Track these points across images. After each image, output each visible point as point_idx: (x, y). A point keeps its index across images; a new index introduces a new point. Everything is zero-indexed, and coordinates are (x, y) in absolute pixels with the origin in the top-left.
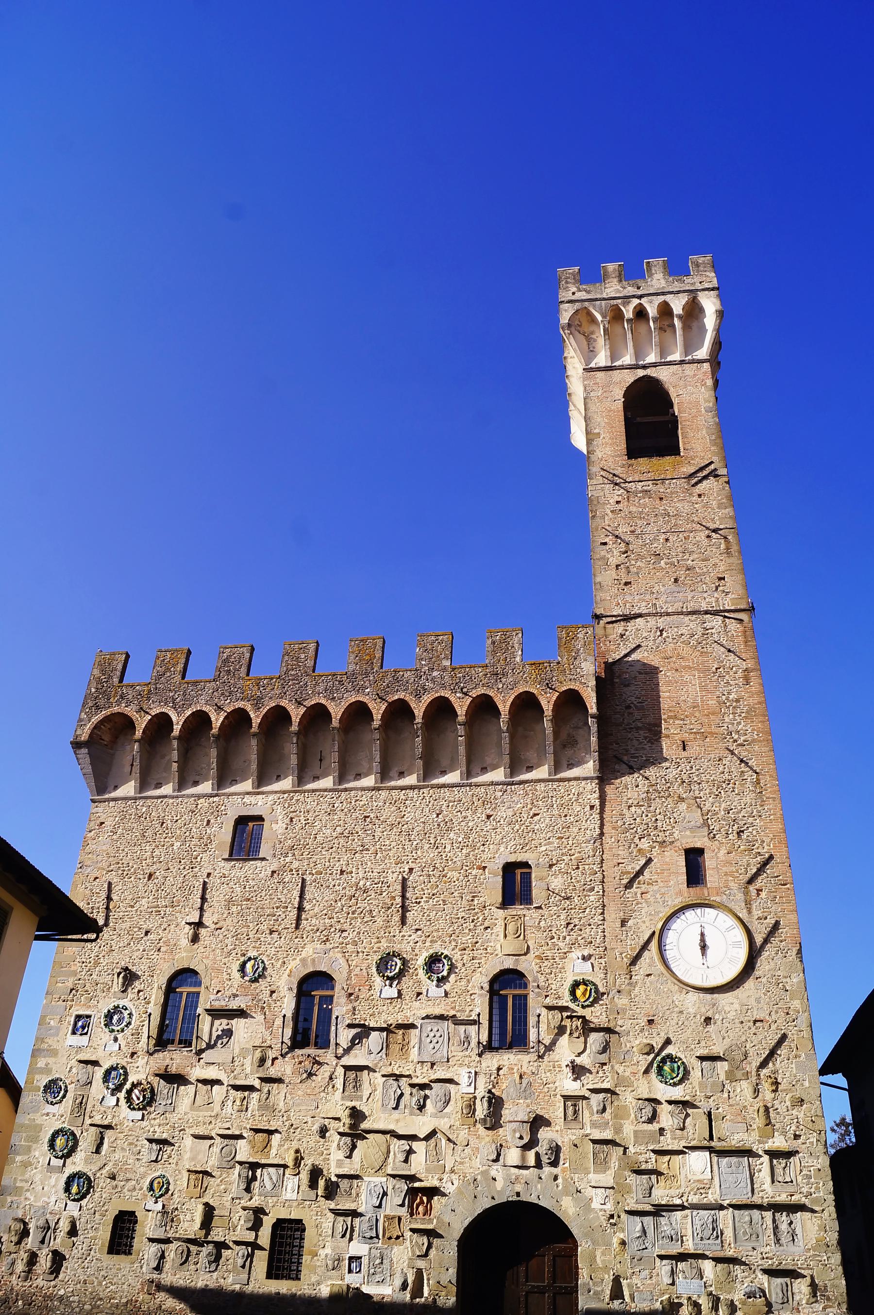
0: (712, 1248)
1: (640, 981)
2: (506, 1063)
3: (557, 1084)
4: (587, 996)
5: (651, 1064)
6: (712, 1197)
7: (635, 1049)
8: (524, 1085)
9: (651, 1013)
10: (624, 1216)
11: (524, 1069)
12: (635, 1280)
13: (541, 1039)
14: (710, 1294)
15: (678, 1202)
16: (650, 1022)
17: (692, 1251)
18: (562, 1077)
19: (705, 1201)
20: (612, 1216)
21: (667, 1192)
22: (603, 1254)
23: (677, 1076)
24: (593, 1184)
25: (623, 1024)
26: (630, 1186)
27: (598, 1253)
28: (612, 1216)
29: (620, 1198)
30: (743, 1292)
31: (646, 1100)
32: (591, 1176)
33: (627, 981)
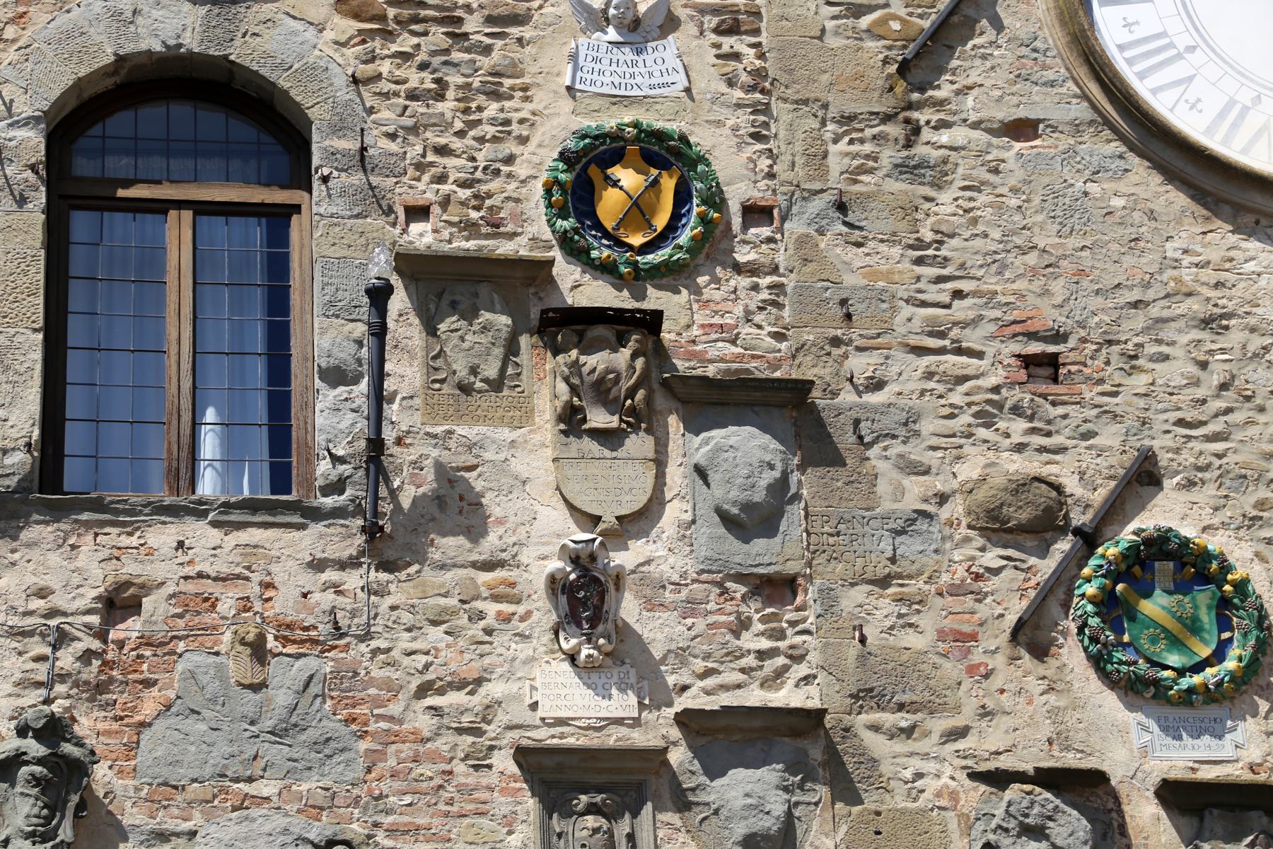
1: (964, 168)
2: (164, 570)
3: (494, 689)
4: (661, 221)
5: (1059, 589)
7: (956, 508)
8: (281, 697)
9: (1049, 317)
11: (284, 604)
13: (388, 434)
16: (1043, 367)
18: (524, 650)
23: (1219, 655)
25: (879, 381)
31: (1051, 779)
33: (889, 156)
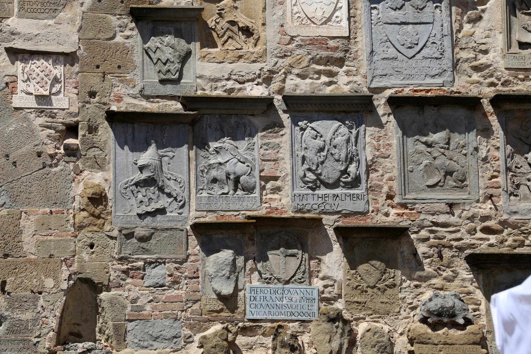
0: (336, 206)
6: (344, 85)
10: (106, 133)
12: (134, 289)
14: (336, 318)
15: (257, 91)
17: (290, 214)
19: (328, 91)
20: (72, 130)
21: (228, 67)
22: (43, 225)
24: (19, 44)
26: (126, 51)
27: (28, 225)
28: (72, 130)
29: (94, 81)
30: (419, 313)
32: (13, 23)
